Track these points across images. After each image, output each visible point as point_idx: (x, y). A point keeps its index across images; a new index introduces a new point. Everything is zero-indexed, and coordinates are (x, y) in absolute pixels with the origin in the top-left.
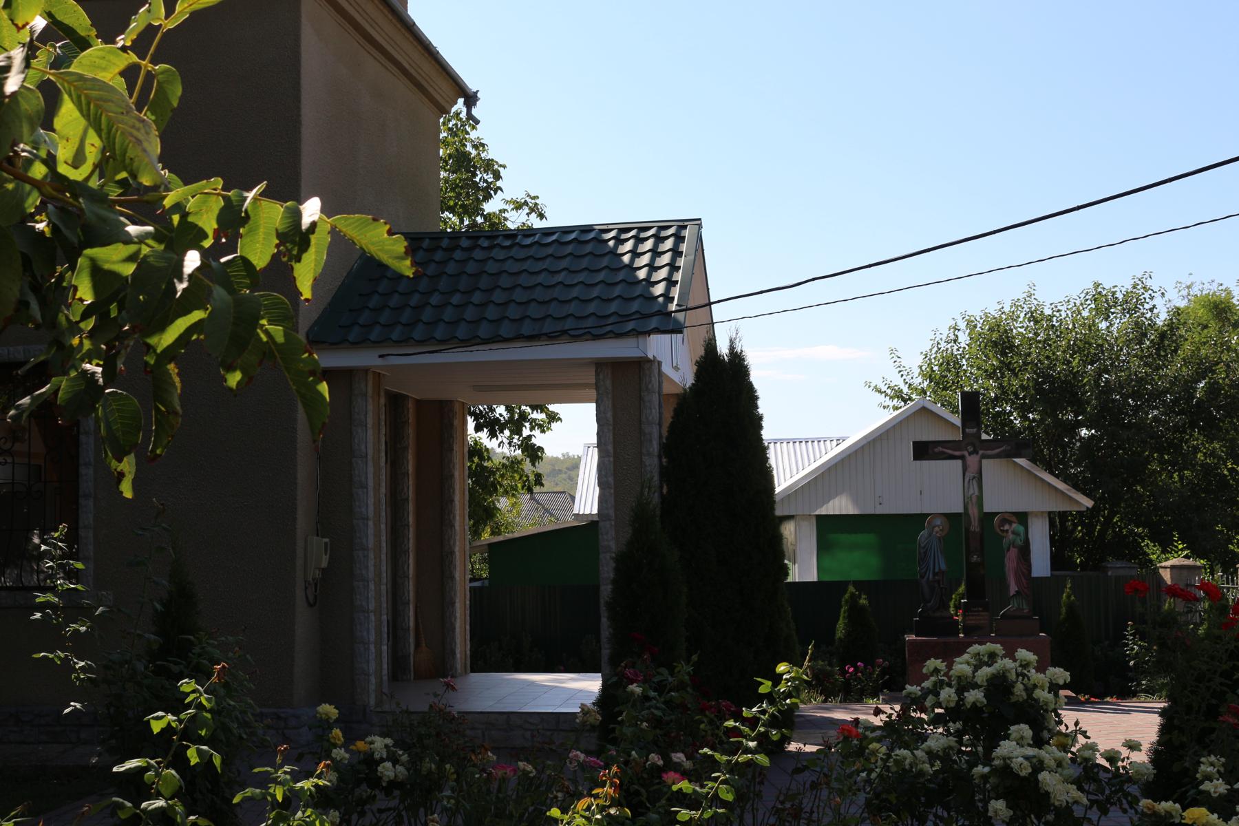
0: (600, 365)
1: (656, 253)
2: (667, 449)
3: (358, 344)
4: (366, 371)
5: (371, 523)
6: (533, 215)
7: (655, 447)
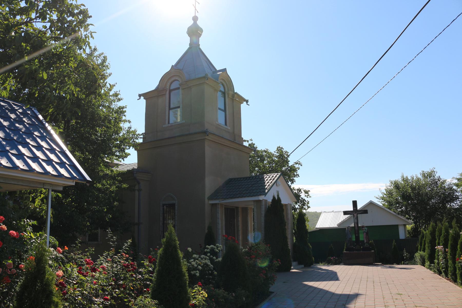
1: (270, 180)
2: (266, 216)
4: (219, 204)
5: (220, 230)
6: (300, 165)
7: (263, 215)
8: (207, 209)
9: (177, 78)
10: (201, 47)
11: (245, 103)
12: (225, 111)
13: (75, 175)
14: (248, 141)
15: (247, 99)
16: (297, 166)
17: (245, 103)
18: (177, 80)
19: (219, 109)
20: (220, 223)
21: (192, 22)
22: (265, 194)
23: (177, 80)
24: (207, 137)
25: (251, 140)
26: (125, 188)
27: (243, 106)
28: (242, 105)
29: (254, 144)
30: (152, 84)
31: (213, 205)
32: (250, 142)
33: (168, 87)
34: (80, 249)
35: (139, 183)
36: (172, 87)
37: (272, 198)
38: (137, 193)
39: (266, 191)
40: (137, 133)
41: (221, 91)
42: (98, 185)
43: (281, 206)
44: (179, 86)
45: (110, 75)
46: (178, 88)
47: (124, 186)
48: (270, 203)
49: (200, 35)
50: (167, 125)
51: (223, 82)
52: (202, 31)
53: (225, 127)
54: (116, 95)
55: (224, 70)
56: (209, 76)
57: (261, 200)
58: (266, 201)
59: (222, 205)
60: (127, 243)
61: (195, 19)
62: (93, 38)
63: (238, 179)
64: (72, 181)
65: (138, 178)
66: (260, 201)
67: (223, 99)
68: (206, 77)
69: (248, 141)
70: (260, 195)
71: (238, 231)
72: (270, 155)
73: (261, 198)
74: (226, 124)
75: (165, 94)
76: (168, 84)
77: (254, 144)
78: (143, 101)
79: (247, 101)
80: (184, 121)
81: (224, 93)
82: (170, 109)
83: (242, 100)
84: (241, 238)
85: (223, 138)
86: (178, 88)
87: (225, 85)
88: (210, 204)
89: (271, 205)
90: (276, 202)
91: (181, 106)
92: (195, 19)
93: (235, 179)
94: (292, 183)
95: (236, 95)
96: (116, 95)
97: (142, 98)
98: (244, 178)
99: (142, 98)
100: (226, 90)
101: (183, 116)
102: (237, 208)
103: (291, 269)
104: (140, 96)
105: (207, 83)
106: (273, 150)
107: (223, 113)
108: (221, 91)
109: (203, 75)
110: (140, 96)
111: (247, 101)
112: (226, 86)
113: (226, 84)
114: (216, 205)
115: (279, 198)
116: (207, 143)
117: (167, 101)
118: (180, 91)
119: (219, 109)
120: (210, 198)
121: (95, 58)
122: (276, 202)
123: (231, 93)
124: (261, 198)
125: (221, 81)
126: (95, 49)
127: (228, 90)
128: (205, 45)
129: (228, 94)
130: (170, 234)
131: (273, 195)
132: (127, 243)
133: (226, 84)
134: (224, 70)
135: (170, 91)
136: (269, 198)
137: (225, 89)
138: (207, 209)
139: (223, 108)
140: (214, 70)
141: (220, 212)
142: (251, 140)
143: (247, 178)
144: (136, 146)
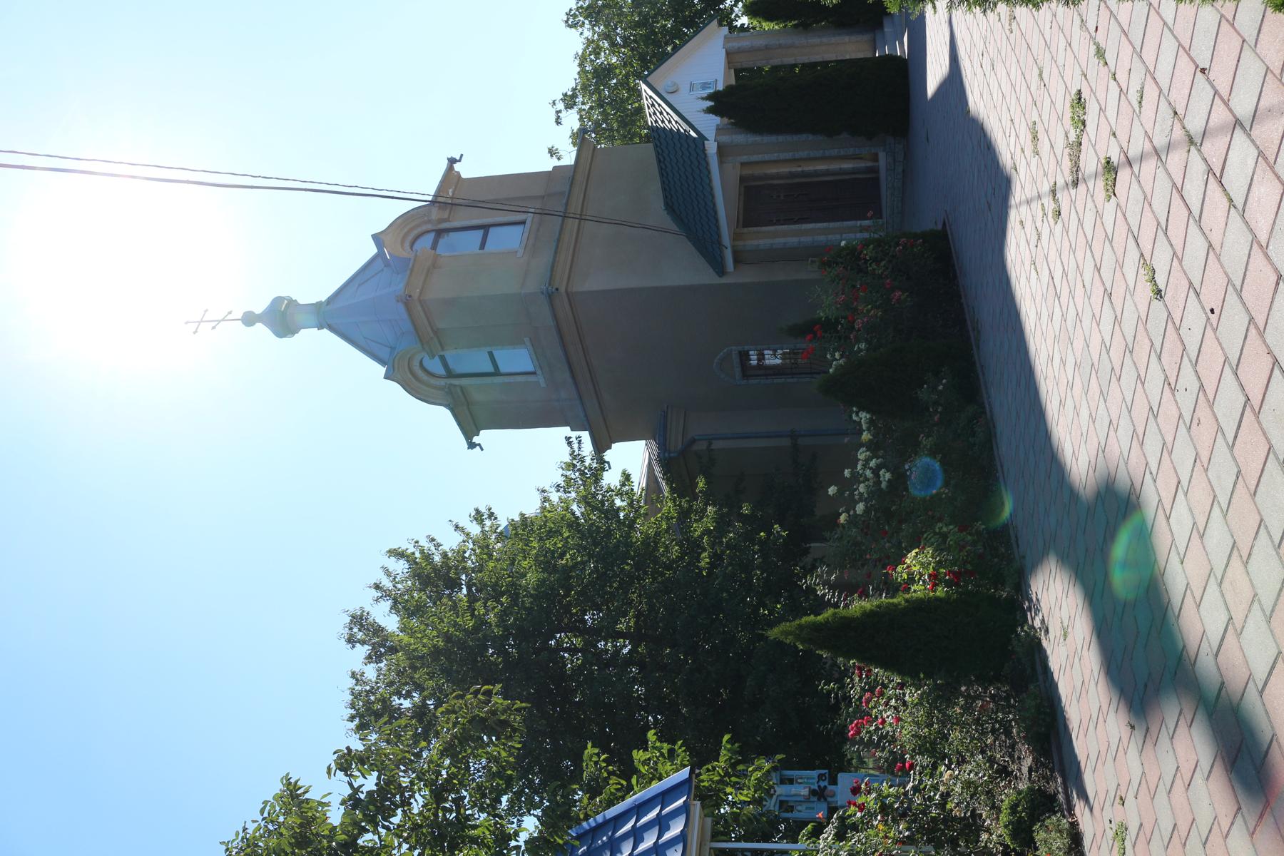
0: (721, 162)
4: (733, 247)
5: (803, 239)
7: (758, 138)
8: (748, 276)
9: (416, 364)
10: (323, 297)
11: (457, 167)
12: (486, 228)
13: (681, 802)
15: (445, 164)
17: (457, 167)
19: (482, 246)
20: (782, 240)
21: (260, 327)
22: (702, 138)
24: (562, 289)
25: (554, 103)
26: (707, 483)
27: (466, 170)
28: (464, 176)
29: (565, 95)
30: (441, 418)
31: (737, 261)
32: (561, 106)
33: (442, 382)
34: (840, 681)
35: (693, 441)
36: (442, 372)
37: (712, 116)
38: (717, 445)
39: (693, 134)
40: (568, 459)
41: (434, 247)
42: (702, 564)
43: (729, 90)
44: (437, 358)
45: (433, 540)
46: (443, 359)
47: (701, 485)
48: (726, 120)
49: (292, 303)
50: (541, 379)
52: (278, 301)
54: (478, 517)
55: (376, 238)
57: (719, 147)
58: (719, 130)
59: (736, 237)
60: (824, 595)
61: (249, 319)
62: (359, 620)
63: (663, 183)
64: (692, 808)
65: (680, 446)
66: (721, 149)
67: (452, 234)
68: (407, 301)
70: (704, 150)
71: (804, 174)
72: (593, 48)
74: (523, 223)
75: (461, 388)
76: (433, 381)
77: (565, 95)
78: (485, 436)
79: (452, 161)
81: (440, 233)
82: (497, 373)
83: (450, 175)
84: (821, 167)
85: (559, 240)
86: (443, 359)
87: (416, 232)
90: (721, 103)
91: (489, 349)
92: (249, 319)
93: (664, 190)
95: (440, 199)
96: (478, 517)
97: (476, 439)
98: (661, 169)
99: (476, 439)
100: (429, 227)
101: (515, 342)
103: (900, 59)
104: (472, 445)
106: (576, 41)
107: (492, 230)
108: (434, 247)
109: (401, 307)
110: (472, 445)
111: (452, 161)
112: (419, 230)
113: (412, 229)
118: (449, 354)
119: (482, 246)
120: (721, 271)
121: (399, 586)
122: (721, 103)
124: (711, 148)
125: (407, 245)
126: (377, 587)
127: (429, 221)
129: (441, 221)
130: (787, 633)
131: (702, 114)
133: (412, 229)
134: (376, 238)
135: (450, 374)
136: (709, 125)
137: (428, 232)
138: (748, 276)
139: (480, 233)
140: (379, 261)
141: (755, 242)
142: (554, 103)
143: (658, 154)
144: (601, 447)
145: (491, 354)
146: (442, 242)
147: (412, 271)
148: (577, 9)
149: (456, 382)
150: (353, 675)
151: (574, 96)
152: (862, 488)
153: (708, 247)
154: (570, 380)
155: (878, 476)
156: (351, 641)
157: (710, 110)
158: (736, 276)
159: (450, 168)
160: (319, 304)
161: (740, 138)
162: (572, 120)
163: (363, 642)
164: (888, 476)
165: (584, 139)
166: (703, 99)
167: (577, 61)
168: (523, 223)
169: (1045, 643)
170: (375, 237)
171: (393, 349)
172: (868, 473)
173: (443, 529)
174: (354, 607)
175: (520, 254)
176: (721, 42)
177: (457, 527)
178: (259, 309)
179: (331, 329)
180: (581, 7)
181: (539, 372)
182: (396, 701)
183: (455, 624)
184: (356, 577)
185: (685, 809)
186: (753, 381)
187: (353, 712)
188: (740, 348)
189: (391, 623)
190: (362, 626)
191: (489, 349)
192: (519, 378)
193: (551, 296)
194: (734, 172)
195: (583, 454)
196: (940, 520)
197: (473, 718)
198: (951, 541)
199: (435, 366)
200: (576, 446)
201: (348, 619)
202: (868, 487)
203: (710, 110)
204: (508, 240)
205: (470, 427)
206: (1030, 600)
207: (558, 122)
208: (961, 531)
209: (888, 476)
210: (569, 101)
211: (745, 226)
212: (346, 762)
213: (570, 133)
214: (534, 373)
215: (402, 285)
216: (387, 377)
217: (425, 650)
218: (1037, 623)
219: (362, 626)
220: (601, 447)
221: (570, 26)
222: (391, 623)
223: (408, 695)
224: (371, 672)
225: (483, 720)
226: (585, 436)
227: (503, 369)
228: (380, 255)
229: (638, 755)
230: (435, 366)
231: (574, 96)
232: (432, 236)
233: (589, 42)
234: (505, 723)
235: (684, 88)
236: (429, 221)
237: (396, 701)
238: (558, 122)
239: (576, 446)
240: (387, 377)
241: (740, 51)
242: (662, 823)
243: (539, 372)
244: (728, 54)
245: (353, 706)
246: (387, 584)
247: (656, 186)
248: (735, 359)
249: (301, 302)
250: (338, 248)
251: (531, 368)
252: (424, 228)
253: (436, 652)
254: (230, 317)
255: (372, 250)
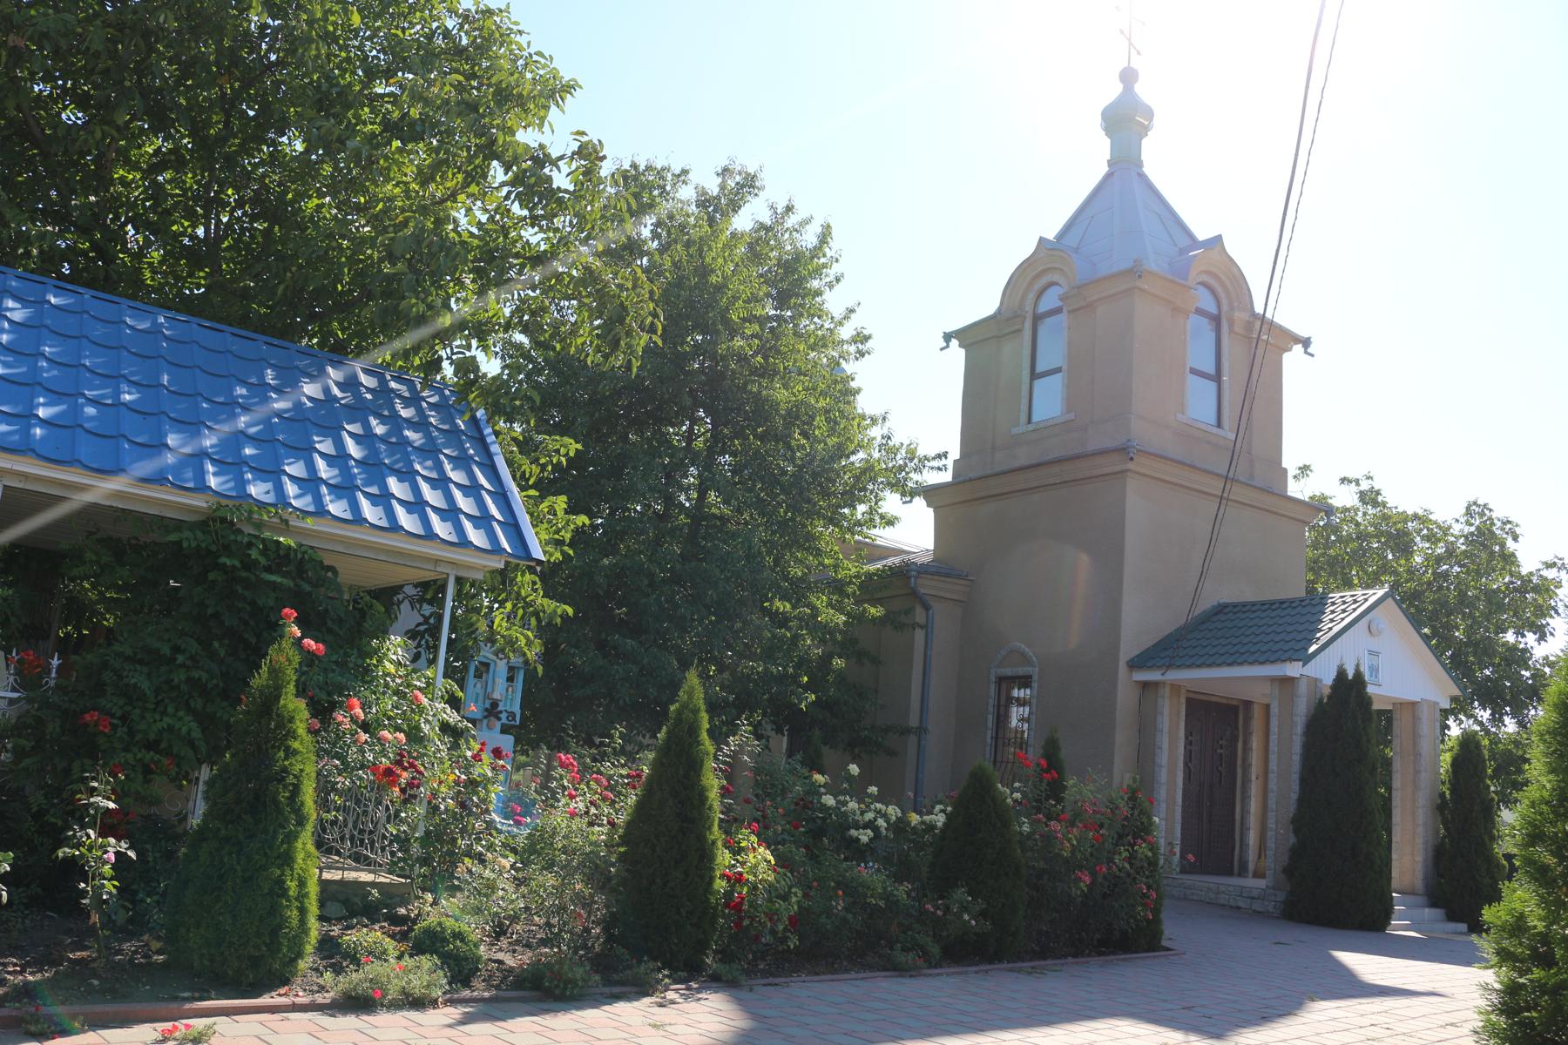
0: (1272, 679)
3: (1150, 668)
7: (1299, 729)
9: (1055, 277)
10: (1147, 170)
11: (1298, 348)
12: (1217, 378)
13: (505, 545)
14: (1358, 484)
15: (1304, 334)
16: (1551, 574)
17: (1298, 348)
18: (1056, 284)
19: (1194, 371)
20: (1165, 746)
21: (1117, 89)
22: (1307, 659)
23: (1056, 284)
24: (1131, 465)
25: (1369, 478)
26: (874, 619)
27: (1292, 360)
28: (1286, 357)
29: (1378, 493)
30: (982, 300)
31: (1145, 685)
32: (1365, 486)
33: (1029, 308)
34: (623, 752)
35: (927, 608)
36: (1042, 308)
37: (1333, 675)
38: (919, 635)
40: (921, 452)
41: (1200, 312)
42: (778, 603)
43: (1365, 701)
45: (838, 280)
46: (1058, 311)
47: (873, 610)
48: (1327, 691)
49: (1145, 130)
50: (1022, 428)
51: (1212, 282)
52: (1150, 114)
53: (1216, 430)
54: (861, 338)
55: (1218, 239)
56: (1152, 265)
57: (1293, 679)
58: (1315, 682)
59: (1176, 688)
60: (728, 745)
61: (1128, 77)
62: (749, 184)
63: (1254, 604)
64: (496, 557)
66: (1288, 682)
67: (1213, 335)
68: (1135, 272)
69: (1358, 484)
70: (1291, 660)
73: (1293, 669)
74: (1219, 425)
75: (1020, 331)
76: (1031, 296)
77: (1378, 493)
78: (957, 354)
79: (1306, 343)
80: (1072, 416)
81: (1216, 320)
82: (1034, 376)
84: (1254, 806)
85: (1192, 467)
86: (1058, 311)
87: (1219, 290)
88: (1137, 682)
89: (1329, 697)
90: (1350, 688)
91: (1065, 368)
92: (1128, 77)
93: (1244, 605)
94: (1542, 638)
96: (861, 338)
97: (954, 343)
98: (1272, 603)
99: (954, 343)
100: (1225, 308)
101: (1070, 401)
102: (1248, 704)
104: (948, 337)
105: (1144, 291)
106: (1448, 511)
107: (1213, 386)
108: (1200, 312)
110: (948, 337)
111: (1306, 343)
112: (1222, 295)
114: (1155, 685)
115: (1359, 679)
116: (1132, 486)
117: (1027, 352)
118: (1062, 318)
119: (1194, 371)
120: (1136, 664)
121: (787, 236)
122: (1350, 688)
123: (1240, 316)
124: (1293, 669)
125: (1205, 278)
126: (789, 209)
128: (1159, 161)
129: (1231, 322)
130: (690, 694)
132: (728, 745)
134: (1218, 239)
135: (1037, 319)
136: (1322, 670)
139: (1211, 370)
140: (1183, 242)
141: (1166, 711)
142: (1369, 478)
143: (1292, 601)
144: (931, 494)
145: (1057, 370)
146: (1205, 321)
147: (1172, 281)
148: (1490, 518)
149: (1028, 325)
150: (685, 172)
151: (1375, 504)
152: (853, 805)
153: (1167, 651)
154: (1017, 464)
155: (865, 827)
156: (725, 172)
157: (1341, 673)
158: (1126, 683)
159: (1297, 340)
160: (1140, 164)
161: (1302, 708)
162: (1344, 498)
163: (722, 187)
164: (864, 839)
165: (1320, 510)
166: (1358, 665)
167: (1421, 513)
168: (1219, 425)
169: (647, 1000)
170: (1219, 239)
171: (1076, 250)
172: (870, 816)
173: (851, 294)
174: (765, 179)
175: (1179, 416)
176: (1432, 698)
177: (852, 311)
178: (1140, 89)
179: (1108, 176)
180: (1493, 524)
181: (1031, 427)
182: (650, 220)
183: (735, 298)
184: (804, 180)
185: (497, 550)
186: (993, 686)
187: (642, 168)
188: (1035, 678)
189: (743, 221)
190: (743, 186)
191: (1065, 368)
192: (1025, 401)
193: (1124, 451)
194: (1258, 694)
195: (925, 471)
196: (806, 895)
197: (624, 308)
198: (780, 904)
199: (1050, 301)
200: (935, 463)
201: (751, 171)
202: (854, 813)
203: (1341, 673)
204: (1199, 403)
205: (971, 338)
206: (699, 991)
207: (1344, 480)
208: (791, 918)
209: (864, 839)
210: (1370, 497)
211: (1189, 701)
212: (589, 154)
213: (1327, 493)
214: (1029, 421)
215: (1153, 267)
216: (1042, 240)
217: (708, 260)
218: (671, 995)
219: (743, 186)
220: (931, 494)
221: (1468, 508)
222: (743, 221)
223: (655, 235)
224: (686, 193)
225: (621, 321)
226: (946, 477)
227: (1037, 383)
228: (1194, 242)
229: (561, 502)
230: (1050, 301)
231: (1375, 504)
232: (1213, 310)
233: (1446, 530)
234: (615, 344)
235: (1373, 644)
236: (1232, 308)
237: (650, 220)
238: (1344, 480)
239: (935, 463)
240: (1042, 240)
241: (1415, 719)
242: (483, 520)
243: (1031, 427)
244: (1413, 704)
245: (649, 168)
246: (791, 221)
247: (1249, 595)
248: (1021, 671)
249: (1144, 141)
250: (1210, 190)
251: (1035, 418)
252: (1224, 302)
253: (704, 271)
254: (1133, 52)
255: (1201, 235)
